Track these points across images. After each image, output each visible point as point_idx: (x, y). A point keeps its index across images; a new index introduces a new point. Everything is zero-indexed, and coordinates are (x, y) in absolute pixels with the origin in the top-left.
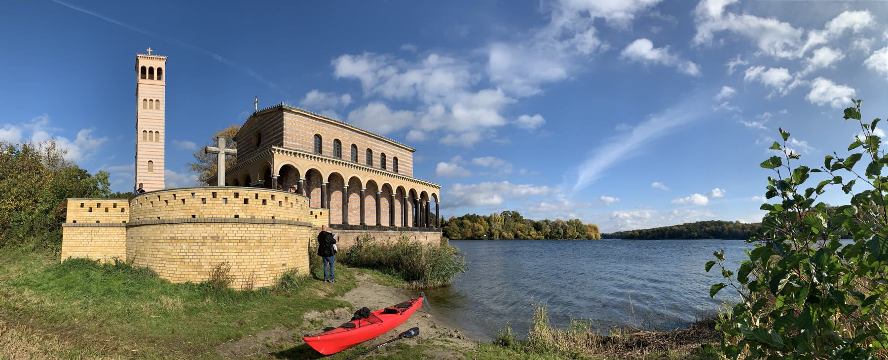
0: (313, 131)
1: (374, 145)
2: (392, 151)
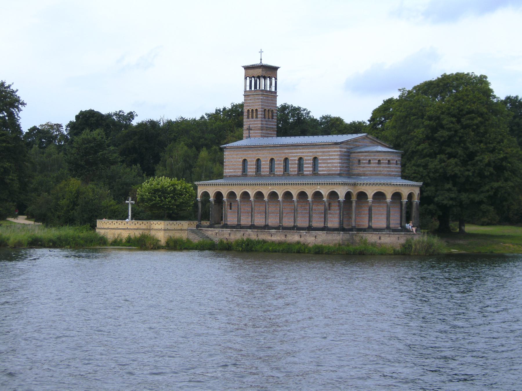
0: (242, 158)
1: (291, 153)
2: (311, 152)
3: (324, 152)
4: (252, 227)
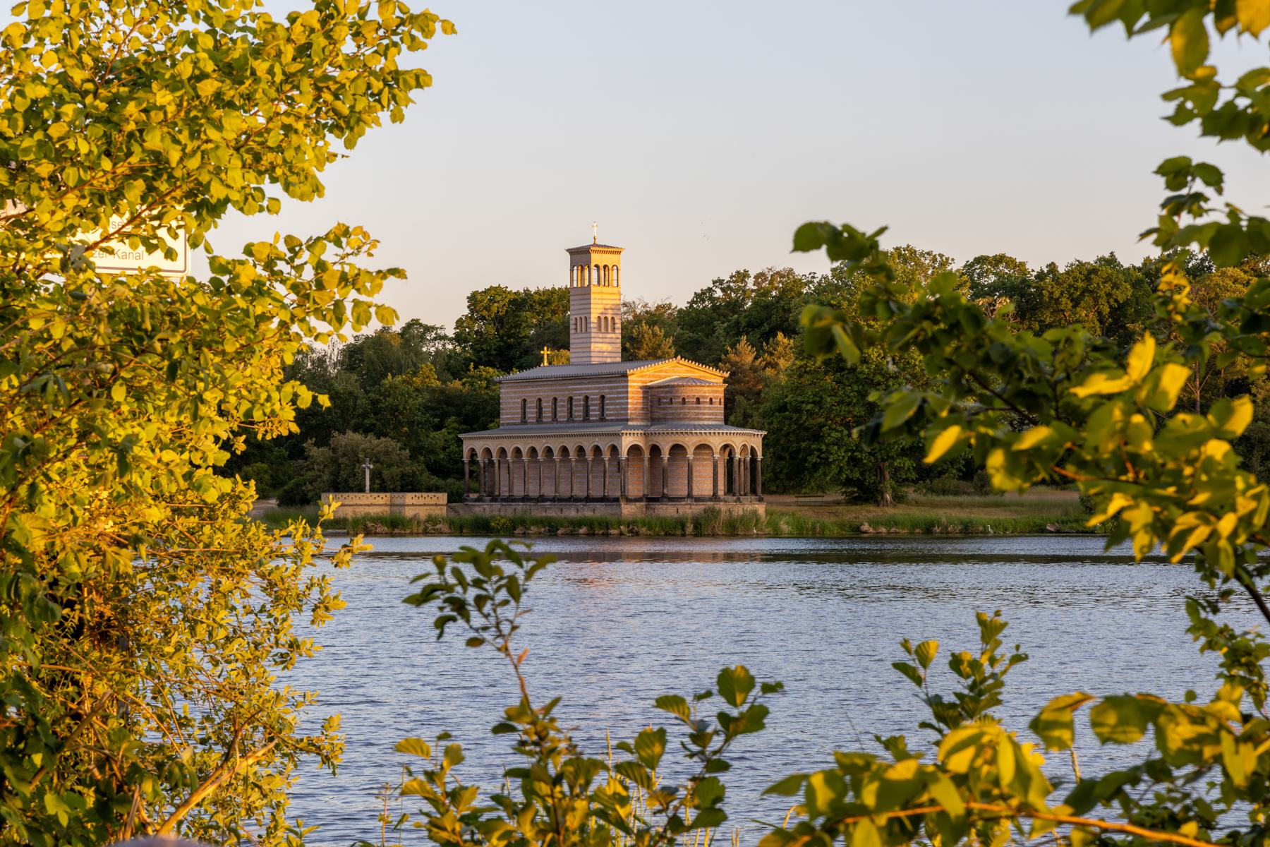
3: (611, 388)
4: (525, 499)
